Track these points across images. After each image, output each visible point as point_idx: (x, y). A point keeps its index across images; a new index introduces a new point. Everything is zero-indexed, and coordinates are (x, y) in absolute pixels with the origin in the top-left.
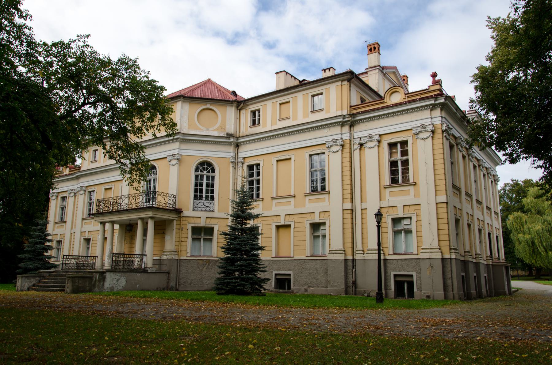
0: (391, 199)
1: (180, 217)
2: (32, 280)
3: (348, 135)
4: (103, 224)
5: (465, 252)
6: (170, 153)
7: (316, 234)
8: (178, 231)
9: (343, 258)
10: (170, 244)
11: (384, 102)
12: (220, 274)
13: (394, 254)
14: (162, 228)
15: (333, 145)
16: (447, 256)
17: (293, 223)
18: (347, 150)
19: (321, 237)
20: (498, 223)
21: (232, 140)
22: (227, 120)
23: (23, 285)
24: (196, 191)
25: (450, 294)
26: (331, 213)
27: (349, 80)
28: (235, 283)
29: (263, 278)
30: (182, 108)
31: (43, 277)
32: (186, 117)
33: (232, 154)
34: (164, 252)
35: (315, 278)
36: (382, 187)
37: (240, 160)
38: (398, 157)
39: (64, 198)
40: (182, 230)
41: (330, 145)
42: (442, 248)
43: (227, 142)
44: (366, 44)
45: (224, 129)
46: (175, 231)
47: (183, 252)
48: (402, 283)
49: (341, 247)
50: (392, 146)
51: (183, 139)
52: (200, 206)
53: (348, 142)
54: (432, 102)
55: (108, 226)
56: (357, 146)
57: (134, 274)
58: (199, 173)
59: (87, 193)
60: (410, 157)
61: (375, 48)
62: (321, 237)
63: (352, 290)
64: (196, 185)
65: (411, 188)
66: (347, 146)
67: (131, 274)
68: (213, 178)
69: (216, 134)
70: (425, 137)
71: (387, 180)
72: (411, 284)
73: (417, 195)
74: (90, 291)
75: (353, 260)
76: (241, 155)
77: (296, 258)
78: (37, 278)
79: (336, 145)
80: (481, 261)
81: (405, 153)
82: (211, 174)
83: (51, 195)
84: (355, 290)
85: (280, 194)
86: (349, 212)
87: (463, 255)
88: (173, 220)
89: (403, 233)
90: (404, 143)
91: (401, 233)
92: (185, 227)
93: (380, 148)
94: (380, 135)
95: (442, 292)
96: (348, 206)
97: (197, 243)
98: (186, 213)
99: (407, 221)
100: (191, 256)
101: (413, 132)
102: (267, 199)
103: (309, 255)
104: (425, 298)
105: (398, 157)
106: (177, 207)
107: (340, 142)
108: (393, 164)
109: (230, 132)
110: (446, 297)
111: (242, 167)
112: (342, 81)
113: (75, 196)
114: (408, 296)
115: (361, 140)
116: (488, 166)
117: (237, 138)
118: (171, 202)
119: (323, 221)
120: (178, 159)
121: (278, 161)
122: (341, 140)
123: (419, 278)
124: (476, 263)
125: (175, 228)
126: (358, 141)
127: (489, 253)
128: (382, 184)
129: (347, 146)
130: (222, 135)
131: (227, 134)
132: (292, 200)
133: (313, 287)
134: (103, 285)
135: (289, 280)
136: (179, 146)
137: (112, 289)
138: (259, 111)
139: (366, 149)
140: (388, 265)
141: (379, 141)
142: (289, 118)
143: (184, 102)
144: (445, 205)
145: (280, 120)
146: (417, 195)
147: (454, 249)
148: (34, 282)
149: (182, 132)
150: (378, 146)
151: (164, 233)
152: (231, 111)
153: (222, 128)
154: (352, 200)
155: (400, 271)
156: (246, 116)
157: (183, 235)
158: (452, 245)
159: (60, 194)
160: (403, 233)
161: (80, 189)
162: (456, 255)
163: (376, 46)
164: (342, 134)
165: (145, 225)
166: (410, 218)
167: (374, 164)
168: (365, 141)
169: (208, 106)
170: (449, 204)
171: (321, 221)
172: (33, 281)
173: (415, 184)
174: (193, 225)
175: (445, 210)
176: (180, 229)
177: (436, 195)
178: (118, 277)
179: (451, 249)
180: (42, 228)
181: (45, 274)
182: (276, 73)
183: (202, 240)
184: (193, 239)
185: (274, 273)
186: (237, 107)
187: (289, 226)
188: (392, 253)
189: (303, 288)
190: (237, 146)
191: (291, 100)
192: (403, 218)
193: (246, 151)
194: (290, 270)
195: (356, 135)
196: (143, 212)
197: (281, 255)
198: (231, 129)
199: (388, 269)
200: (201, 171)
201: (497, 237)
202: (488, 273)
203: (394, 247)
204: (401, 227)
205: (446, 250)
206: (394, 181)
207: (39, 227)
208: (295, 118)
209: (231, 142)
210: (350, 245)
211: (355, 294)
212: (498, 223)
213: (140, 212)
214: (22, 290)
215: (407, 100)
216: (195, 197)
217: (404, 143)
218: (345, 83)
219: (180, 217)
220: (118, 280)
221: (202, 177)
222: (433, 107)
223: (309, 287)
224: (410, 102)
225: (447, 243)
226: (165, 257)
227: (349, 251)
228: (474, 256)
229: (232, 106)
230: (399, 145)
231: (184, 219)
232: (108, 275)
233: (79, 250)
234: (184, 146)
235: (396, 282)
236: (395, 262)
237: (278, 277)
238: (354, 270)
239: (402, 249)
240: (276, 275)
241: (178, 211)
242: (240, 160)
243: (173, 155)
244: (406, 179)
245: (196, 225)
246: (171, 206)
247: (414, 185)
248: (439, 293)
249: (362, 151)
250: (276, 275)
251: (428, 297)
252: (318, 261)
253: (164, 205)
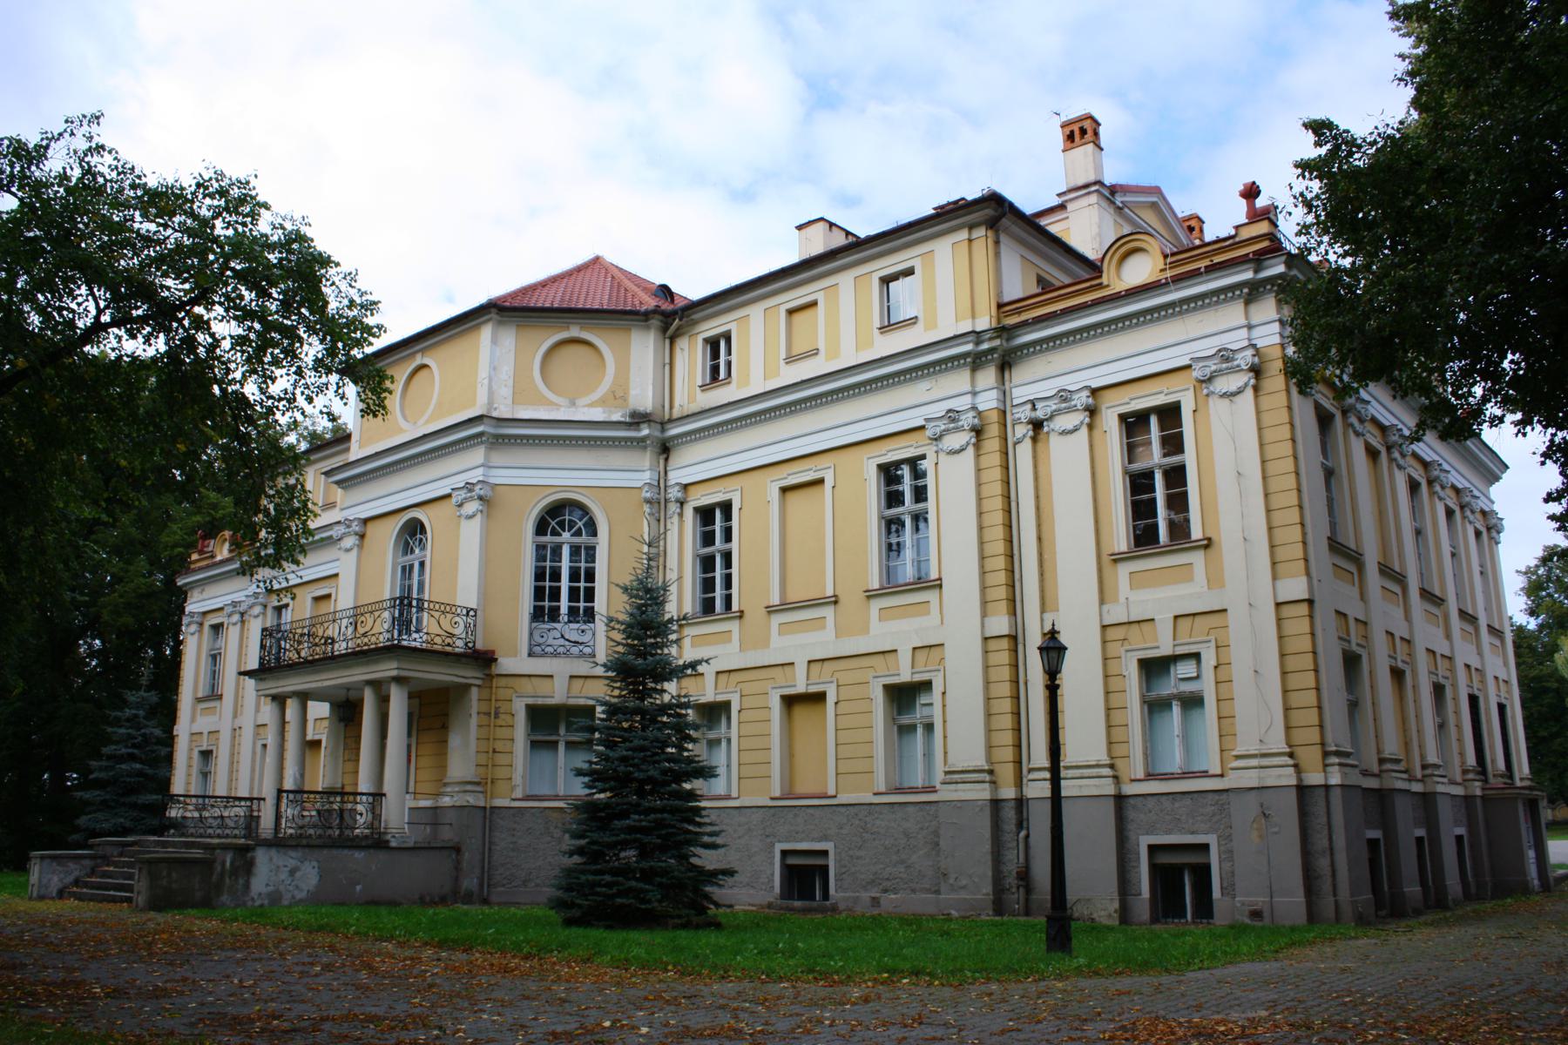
0: (1136, 596)
1: (490, 677)
2: (72, 865)
3: (994, 394)
4: (280, 700)
5: (1382, 761)
6: (459, 481)
7: (905, 720)
8: (485, 720)
9: (987, 795)
10: (462, 759)
11: (1100, 286)
12: (571, 854)
13: (1150, 776)
14: (433, 713)
15: (947, 431)
16: (1314, 778)
17: (834, 686)
18: (992, 444)
19: (920, 730)
20: (1506, 664)
21: (645, 432)
22: (635, 370)
23: (45, 881)
24: (539, 593)
25: (1327, 905)
26: (948, 652)
27: (992, 224)
28: (609, 885)
29: (710, 867)
30: (494, 341)
31: (104, 857)
32: (506, 371)
33: (647, 477)
34: (445, 785)
35: (902, 862)
36: (1106, 560)
37: (674, 493)
38: (1154, 456)
39: (217, 628)
40: (497, 715)
41: (938, 430)
42: (1299, 751)
43: (631, 439)
44: (1058, 122)
45: (624, 398)
46: (474, 721)
47: (502, 786)
48: (1178, 870)
49: (980, 761)
50: (1134, 423)
51: (497, 437)
52: (550, 641)
53: (994, 416)
54: (1248, 275)
55: (292, 708)
56: (1022, 430)
57: (346, 852)
58: (548, 538)
59: (270, 611)
60: (1189, 457)
61: (1083, 132)
62: (920, 730)
63: (1015, 898)
64: (539, 575)
65: (1197, 559)
66: (993, 430)
67: (335, 852)
68: (591, 551)
69: (597, 414)
70: (1233, 388)
71: (1120, 536)
72: (1202, 874)
73: (1215, 580)
74: (207, 903)
75: (1021, 802)
76: (677, 476)
77: (844, 798)
78: (87, 862)
79: (958, 429)
80: (1440, 789)
81: (1173, 444)
82: (584, 539)
83: (185, 620)
84: (1027, 900)
85: (792, 597)
86: (1005, 644)
87: (1375, 769)
88: (468, 686)
89: (1176, 709)
90: (1169, 414)
91: (1170, 706)
92: (504, 707)
93: (1096, 433)
94: (1095, 392)
95: (1300, 898)
96: (1000, 624)
97: (545, 756)
98: (507, 664)
99: (1185, 669)
100: (527, 798)
101: (1195, 374)
102: (755, 613)
103: (882, 789)
104: (1247, 921)
105: (1154, 456)
106: (479, 646)
107: (968, 420)
108: (1139, 483)
109: (641, 409)
110: (1312, 916)
111: (681, 515)
112: (971, 227)
113: (243, 622)
114: (1196, 915)
115: (1034, 408)
116: (1461, 483)
117: (663, 425)
118: (459, 630)
119: (925, 677)
120: (481, 498)
121: (785, 490)
122: (972, 414)
123: (1228, 855)
124: (1424, 794)
125: (474, 711)
126: (1025, 413)
127: (1471, 760)
128: (1106, 550)
129: (993, 430)
130: (616, 417)
131: (634, 414)
132: (828, 612)
133: (895, 891)
134: (247, 886)
135: (824, 870)
136: (487, 457)
137: (275, 898)
138: (727, 337)
139: (1054, 440)
140: (1131, 814)
141: (1092, 411)
142: (816, 352)
143: (500, 323)
144: (1303, 609)
145: (791, 359)
146: (1215, 580)
147: (1338, 754)
148: (76, 873)
149: (495, 414)
150: (1091, 427)
151: (445, 727)
152: (644, 346)
153: (617, 395)
154: (1013, 605)
155: (1169, 832)
156: (691, 356)
157: (501, 733)
158: (1329, 738)
159: (209, 616)
160: (1176, 709)
161: (252, 600)
162: (1344, 775)
163: (1087, 124)
164: (974, 394)
165: (383, 701)
166: (1197, 656)
167: (1078, 483)
168: (1049, 410)
169: (574, 332)
170: (1317, 605)
171: (918, 678)
172: (75, 870)
173: (1207, 544)
174: (530, 701)
175: (1305, 626)
176: (493, 714)
177: (1275, 578)
178: (292, 863)
179: (1326, 754)
180: (136, 716)
181: (109, 850)
182: (800, 228)
183: (561, 747)
184: (534, 745)
185: (779, 847)
186: (664, 330)
187: (820, 697)
188: (1141, 775)
189: (865, 896)
190: (665, 449)
191: (820, 297)
192: (1176, 659)
193: (690, 465)
194: (825, 838)
195: (1020, 394)
196: (376, 662)
197: (800, 789)
198: (643, 397)
199: (1131, 826)
200: (555, 533)
201: (1501, 707)
202: (1471, 825)
203: (1149, 754)
204: (1169, 686)
205: (1311, 757)
206: (1144, 537)
207: (128, 712)
208: (834, 354)
209: (643, 439)
210: (1008, 754)
211: (1027, 913)
212: (1506, 664)
213: (367, 663)
214: (41, 898)
215: (1169, 274)
216: (538, 614)
217: (1169, 414)
218: (980, 232)
219: (490, 677)
220: (292, 872)
221: (557, 551)
222: (1252, 293)
223: (885, 891)
224: (1178, 280)
225: (1314, 735)
226: (446, 801)
227: (1006, 773)
228: (1419, 774)
229: (648, 328)
230: (1154, 420)
231: (503, 682)
232: (262, 857)
234: (498, 458)
235: (1154, 868)
236: (1151, 802)
237: (792, 861)
238: (1023, 834)
239: (1174, 760)
240: (784, 853)
241: (483, 659)
242: (674, 493)
243: (469, 487)
244: (1180, 530)
245: (540, 701)
246: (460, 643)
247: (1206, 547)
248: (1292, 902)
249: (1040, 445)
250: (784, 853)
251: (1256, 914)
252: (911, 809)
253: (438, 640)
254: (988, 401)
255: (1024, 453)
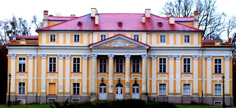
13: (215, 96)
105: (218, 64)
139: (208, 61)
159: (19, 56)
167: (210, 65)
195: (204, 55)
222: (230, 50)
233: (33, 88)
254: (201, 55)
255: (204, 61)
